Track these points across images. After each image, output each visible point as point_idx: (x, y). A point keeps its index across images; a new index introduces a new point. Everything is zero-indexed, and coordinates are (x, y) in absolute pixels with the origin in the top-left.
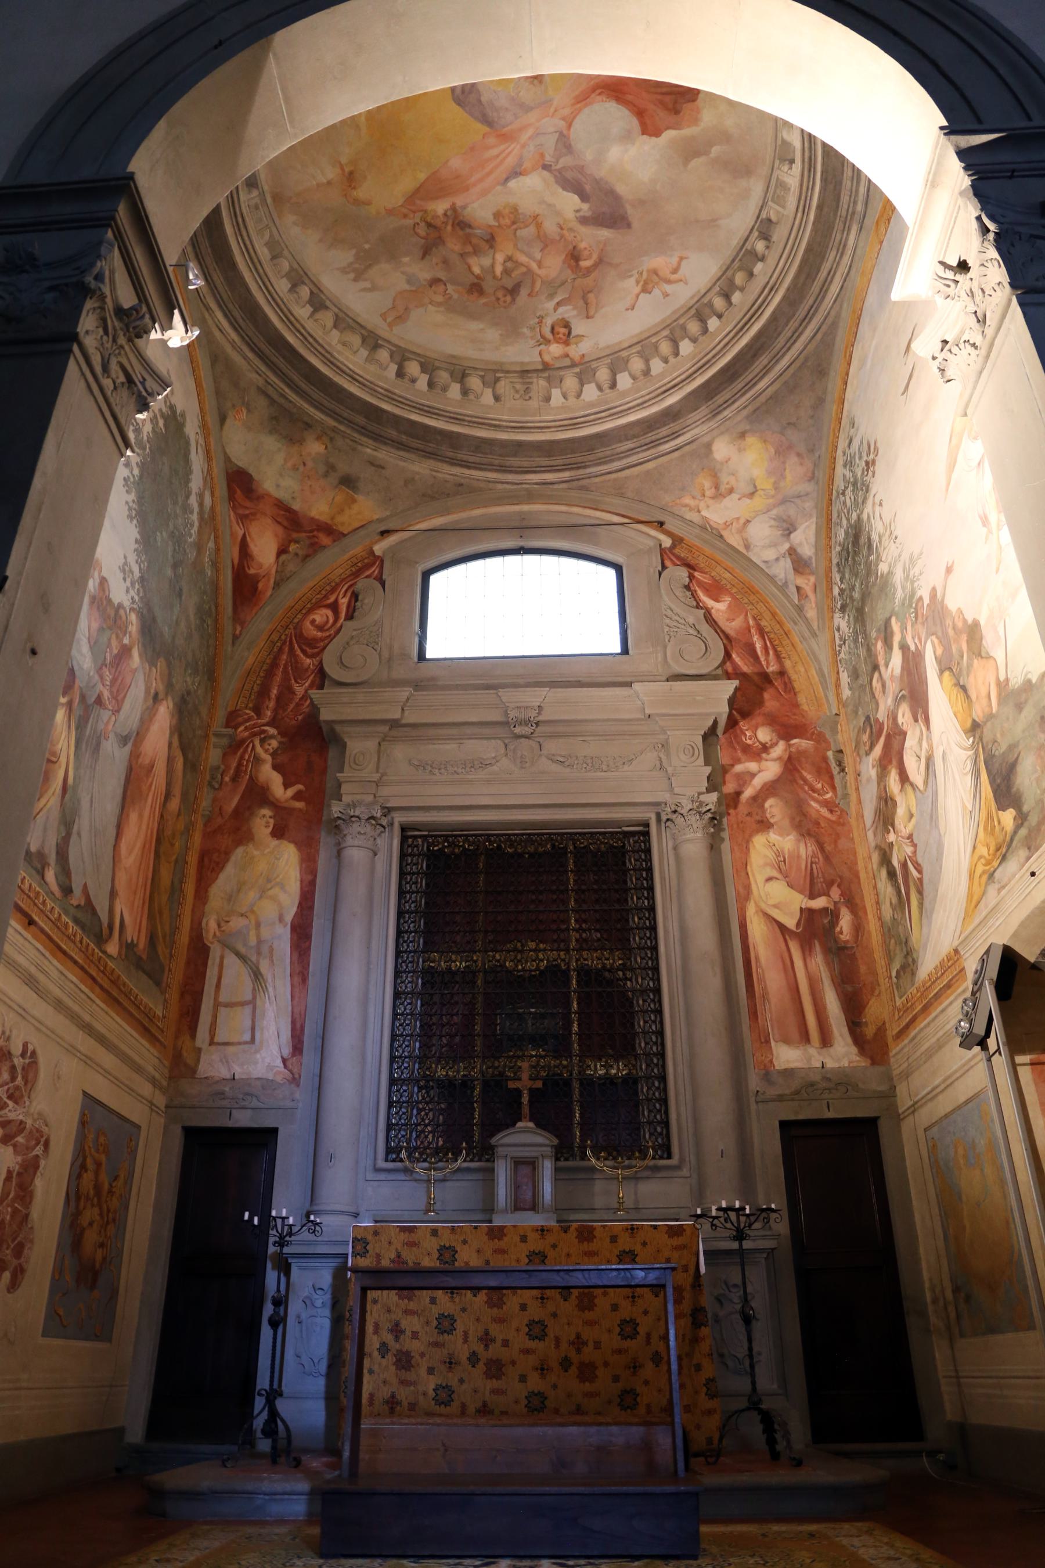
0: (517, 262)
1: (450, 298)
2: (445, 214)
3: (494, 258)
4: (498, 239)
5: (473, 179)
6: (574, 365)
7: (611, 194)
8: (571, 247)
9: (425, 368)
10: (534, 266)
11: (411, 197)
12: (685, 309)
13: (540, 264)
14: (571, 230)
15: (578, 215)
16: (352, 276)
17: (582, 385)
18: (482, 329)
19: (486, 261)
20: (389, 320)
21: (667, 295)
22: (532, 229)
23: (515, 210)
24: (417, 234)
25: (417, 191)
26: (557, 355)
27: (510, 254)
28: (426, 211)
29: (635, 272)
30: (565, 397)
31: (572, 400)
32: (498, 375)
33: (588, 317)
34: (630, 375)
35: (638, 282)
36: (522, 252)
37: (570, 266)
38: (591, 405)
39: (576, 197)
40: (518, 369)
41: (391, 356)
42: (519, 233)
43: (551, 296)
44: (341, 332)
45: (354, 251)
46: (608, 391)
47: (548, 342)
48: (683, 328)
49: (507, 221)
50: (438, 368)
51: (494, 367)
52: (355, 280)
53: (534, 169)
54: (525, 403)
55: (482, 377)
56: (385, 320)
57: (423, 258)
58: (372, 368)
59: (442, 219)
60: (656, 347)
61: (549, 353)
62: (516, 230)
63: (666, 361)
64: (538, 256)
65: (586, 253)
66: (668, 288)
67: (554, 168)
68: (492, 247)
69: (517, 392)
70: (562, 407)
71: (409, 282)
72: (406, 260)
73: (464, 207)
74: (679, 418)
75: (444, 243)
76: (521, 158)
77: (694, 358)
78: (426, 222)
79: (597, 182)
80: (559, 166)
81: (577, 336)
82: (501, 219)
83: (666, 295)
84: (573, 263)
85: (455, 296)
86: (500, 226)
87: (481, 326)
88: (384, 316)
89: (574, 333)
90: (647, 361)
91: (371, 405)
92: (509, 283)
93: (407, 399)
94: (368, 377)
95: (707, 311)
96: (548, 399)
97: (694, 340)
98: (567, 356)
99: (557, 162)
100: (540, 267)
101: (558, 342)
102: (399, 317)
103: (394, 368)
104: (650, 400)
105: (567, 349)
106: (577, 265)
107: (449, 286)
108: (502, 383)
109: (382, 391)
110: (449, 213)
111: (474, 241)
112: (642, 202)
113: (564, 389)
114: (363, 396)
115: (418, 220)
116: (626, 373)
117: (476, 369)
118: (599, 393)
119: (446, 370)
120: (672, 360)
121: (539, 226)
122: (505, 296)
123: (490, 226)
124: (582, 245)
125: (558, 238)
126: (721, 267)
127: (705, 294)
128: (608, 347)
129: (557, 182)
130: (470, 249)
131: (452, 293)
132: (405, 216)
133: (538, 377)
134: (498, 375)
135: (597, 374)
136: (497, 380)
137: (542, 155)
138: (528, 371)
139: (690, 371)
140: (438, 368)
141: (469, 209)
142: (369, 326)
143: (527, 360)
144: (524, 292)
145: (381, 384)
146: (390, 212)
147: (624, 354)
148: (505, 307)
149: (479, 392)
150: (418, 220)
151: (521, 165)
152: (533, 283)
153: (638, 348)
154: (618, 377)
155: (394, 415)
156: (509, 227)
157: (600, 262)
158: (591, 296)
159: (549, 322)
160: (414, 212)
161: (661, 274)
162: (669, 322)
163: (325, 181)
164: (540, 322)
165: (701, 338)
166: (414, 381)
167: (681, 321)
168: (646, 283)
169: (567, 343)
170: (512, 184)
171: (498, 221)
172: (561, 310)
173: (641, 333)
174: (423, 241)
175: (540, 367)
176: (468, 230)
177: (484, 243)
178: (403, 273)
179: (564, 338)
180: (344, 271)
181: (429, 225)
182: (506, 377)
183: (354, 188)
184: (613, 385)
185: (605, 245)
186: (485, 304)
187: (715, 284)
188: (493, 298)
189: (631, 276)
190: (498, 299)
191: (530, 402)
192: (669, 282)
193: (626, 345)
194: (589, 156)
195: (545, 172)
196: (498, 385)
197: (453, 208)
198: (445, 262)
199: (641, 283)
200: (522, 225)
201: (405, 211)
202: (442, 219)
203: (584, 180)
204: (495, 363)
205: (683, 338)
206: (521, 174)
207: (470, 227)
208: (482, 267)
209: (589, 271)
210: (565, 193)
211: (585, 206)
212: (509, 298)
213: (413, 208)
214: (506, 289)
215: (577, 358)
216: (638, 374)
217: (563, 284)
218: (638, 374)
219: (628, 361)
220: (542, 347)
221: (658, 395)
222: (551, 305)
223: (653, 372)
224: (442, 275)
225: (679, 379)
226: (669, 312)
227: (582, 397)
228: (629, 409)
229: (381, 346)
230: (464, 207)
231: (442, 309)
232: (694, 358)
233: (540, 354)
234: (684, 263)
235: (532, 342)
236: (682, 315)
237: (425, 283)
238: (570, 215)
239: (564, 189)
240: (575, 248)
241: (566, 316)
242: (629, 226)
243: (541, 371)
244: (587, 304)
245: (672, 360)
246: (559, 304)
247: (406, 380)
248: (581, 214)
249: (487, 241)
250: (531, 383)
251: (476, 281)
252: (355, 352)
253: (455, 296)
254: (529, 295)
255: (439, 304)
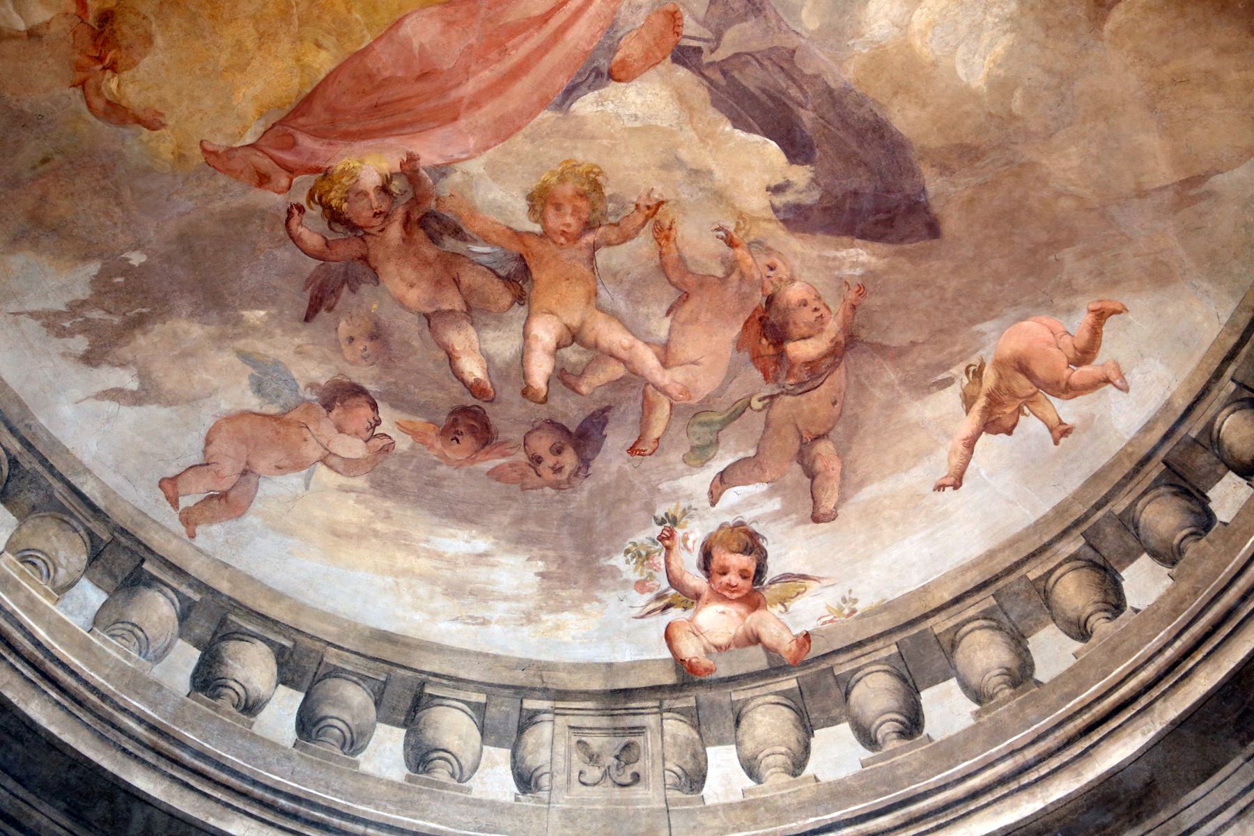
0: (596, 346)
1: (387, 449)
2: (384, 189)
3: (526, 336)
4: (541, 276)
5: (469, 88)
6: (777, 668)
7: (878, 130)
8: (759, 299)
9: (289, 672)
10: (648, 360)
11: (282, 122)
12: (1128, 466)
13: (666, 356)
14: (759, 245)
15: (779, 200)
16: (80, 344)
17: (807, 727)
18: (485, 555)
19: (503, 344)
20: (185, 502)
21: (1066, 432)
22: (643, 244)
23: (593, 186)
24: (296, 240)
25: (305, 104)
26: (722, 640)
27: (574, 320)
28: (326, 174)
29: (957, 370)
30: (751, 768)
31: (775, 781)
32: (530, 704)
33: (816, 519)
34: (965, 686)
35: (968, 401)
36: (613, 315)
37: (756, 358)
38: (840, 792)
39: (773, 145)
40: (597, 685)
41: (183, 617)
42: (602, 255)
43: (700, 454)
44: (22, 518)
45: (94, 268)
46: (894, 744)
47: (692, 599)
48: (1128, 523)
49: (571, 221)
50: (336, 673)
51: (520, 678)
52: (90, 359)
53: (649, 62)
54: (618, 793)
55: (479, 710)
56: (174, 503)
57: (307, 319)
58: (112, 648)
59: (376, 201)
60: (1043, 592)
61: (697, 633)
62: (595, 247)
63: (1081, 631)
64: (661, 327)
65: (807, 316)
66: (1066, 410)
67: (707, 58)
68: (521, 298)
69: (593, 758)
70: (746, 806)
71: (259, 388)
72: (256, 316)
73: (442, 171)
74: (1154, 811)
75: (376, 278)
76: (611, 27)
77: (1176, 612)
78: (326, 207)
79: (833, 98)
80: (720, 55)
81: (787, 577)
82: (551, 213)
83: (1061, 431)
84: (766, 347)
85: (403, 443)
86: (545, 235)
87: (482, 544)
88: (170, 486)
89: (774, 568)
90: (1018, 641)
91: (97, 769)
92: (572, 412)
93: (221, 766)
94: (97, 679)
95: (1203, 460)
96: (695, 779)
97: (1169, 556)
98: (754, 639)
99: (719, 37)
100: (665, 364)
101: (724, 599)
102: (223, 496)
103: (187, 657)
104: (1040, 760)
105: (756, 619)
106: (781, 355)
107: (385, 412)
108: (543, 732)
109: (139, 729)
110: (396, 186)
111: (469, 277)
112: (968, 154)
113: (749, 746)
114: (67, 738)
115: (303, 200)
116: (953, 682)
117: (458, 682)
118: (866, 754)
119: (361, 679)
120: (1101, 626)
121: (663, 234)
122: (559, 452)
123: (519, 235)
124: (795, 293)
125: (720, 272)
126: (1231, 323)
127: (1189, 410)
128: (887, 607)
129: (716, 103)
130: (453, 301)
131: (395, 434)
132: (263, 180)
133: (661, 710)
134: (530, 704)
135: (856, 693)
136: (528, 720)
137: (674, 18)
138: (628, 693)
139: (1169, 653)
140: (336, 673)
141: (456, 178)
142: (120, 515)
143: (625, 655)
144: (616, 440)
145: (136, 704)
146: (216, 159)
147: (940, 624)
148: (557, 486)
149: (467, 759)
150: (303, 200)
151: (613, 50)
152: (647, 408)
153: (986, 601)
154: (926, 696)
155: (173, 817)
156: (577, 237)
157: (847, 344)
158: (824, 448)
159: (695, 533)
160: (291, 171)
161: (1040, 370)
162: (1079, 510)
163: (21, 26)
164: (666, 539)
165: (1191, 548)
166: (251, 707)
167: (1120, 506)
168: (994, 400)
169: (752, 601)
170: (585, 105)
171: (542, 219)
172: (732, 496)
173: (991, 554)
174: (314, 264)
175: (669, 679)
176: (450, 244)
177: (499, 286)
178: (245, 356)
179: (745, 585)
180: (53, 323)
181: (335, 217)
182: (556, 712)
183: (113, 67)
184: (912, 724)
185: (862, 291)
186: (495, 474)
187: (1218, 375)
188: (521, 457)
189: (948, 382)
190: (537, 460)
191: (638, 792)
192: (1068, 390)
193: (948, 597)
194: (810, 21)
195: (682, 72)
196: (530, 738)
197: (410, 170)
198: (377, 334)
199: (981, 402)
200: (613, 235)
201: (264, 163)
202: (376, 201)
203: (793, 92)
204: (525, 665)
205: (1131, 557)
206: (612, 76)
207: (457, 232)
208: (489, 359)
209: (815, 370)
210: (740, 134)
211: (800, 175)
212: (569, 459)
213: (287, 157)
214: (563, 429)
215: (786, 644)
216: (993, 681)
217: (737, 413)
218: (993, 681)
219: (954, 645)
220: (675, 614)
221: (1070, 742)
222: (699, 481)
223: (1043, 673)
224: (364, 375)
225: (1133, 683)
226: (1074, 483)
227: (810, 769)
228: (974, 795)
229: (151, 582)
230: (442, 171)
231: (360, 482)
232: (1176, 612)
233: (668, 637)
234: (1110, 328)
235: (642, 600)
236: (1119, 486)
237: (310, 396)
238: (756, 202)
239: (738, 122)
240: (770, 300)
241: (747, 516)
242: (933, 229)
243: (673, 688)
244: (812, 475)
245: (1101, 626)
246: (723, 480)
247: (226, 704)
248: (789, 197)
249: (508, 280)
250: (640, 730)
251: (469, 401)
252: (64, 589)
253: (403, 443)
254: (632, 450)
255: (350, 467)
